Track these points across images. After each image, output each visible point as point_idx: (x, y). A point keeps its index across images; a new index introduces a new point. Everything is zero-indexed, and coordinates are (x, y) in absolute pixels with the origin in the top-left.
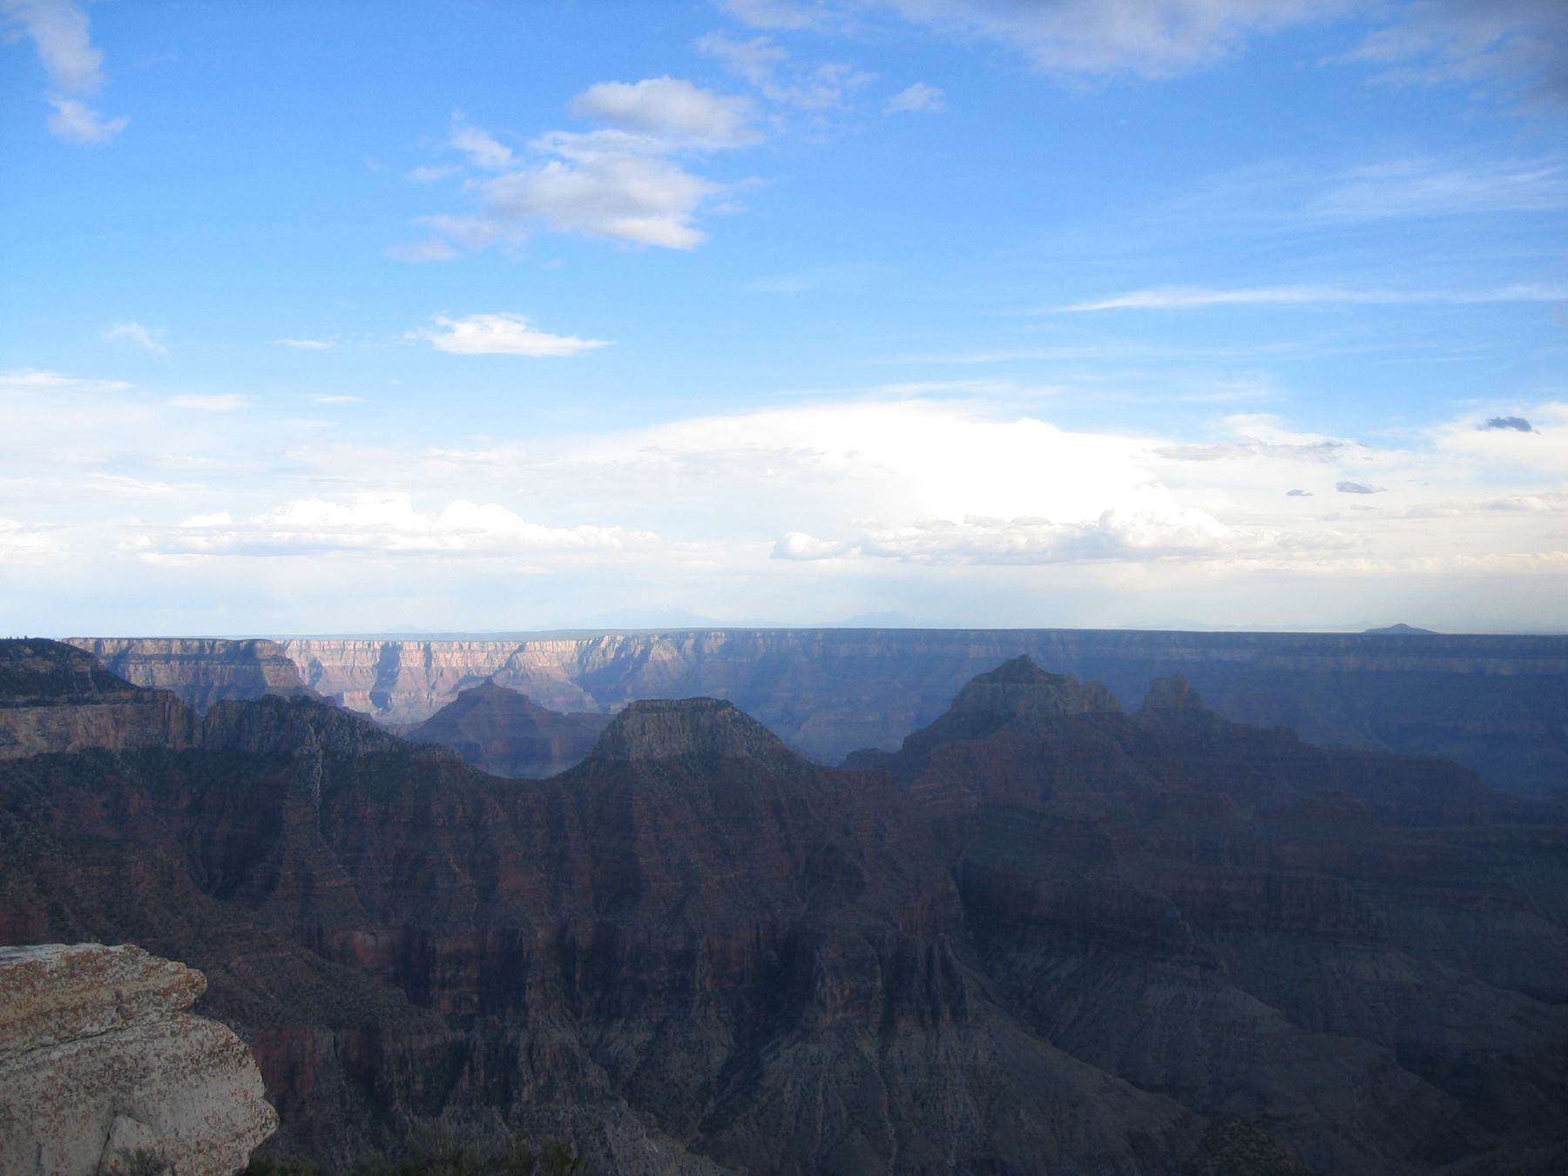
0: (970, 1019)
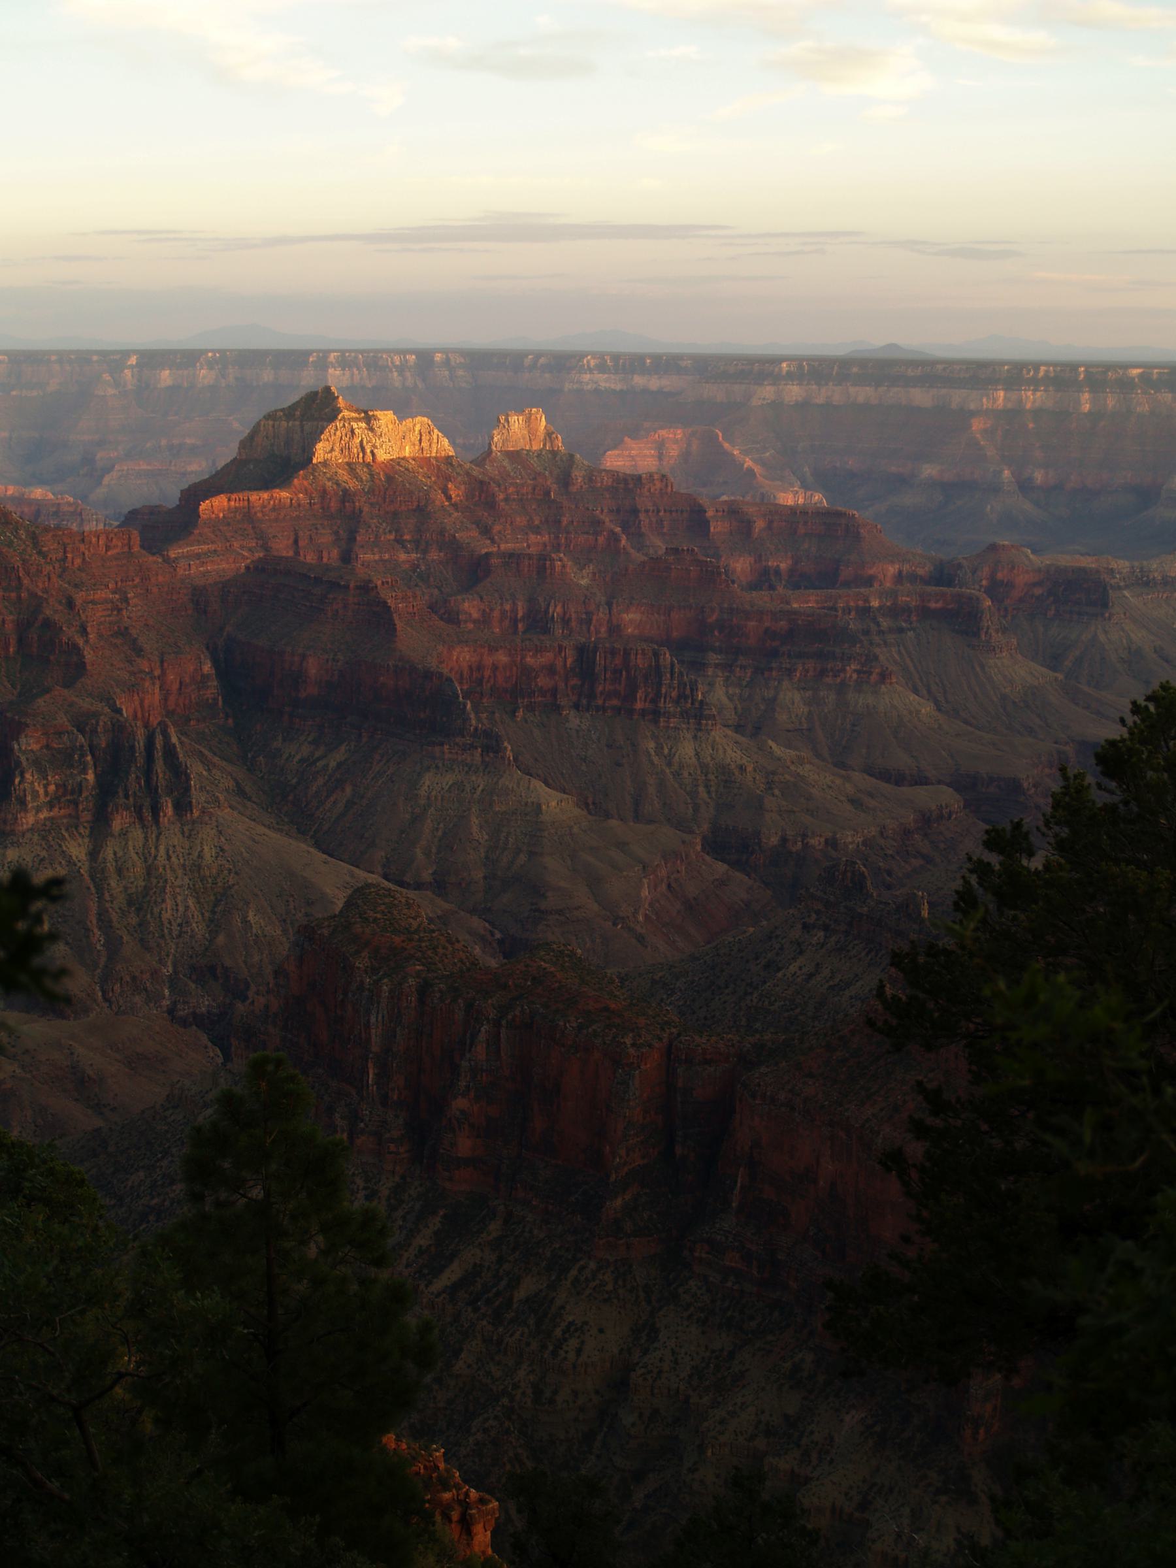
0: (196, 814)
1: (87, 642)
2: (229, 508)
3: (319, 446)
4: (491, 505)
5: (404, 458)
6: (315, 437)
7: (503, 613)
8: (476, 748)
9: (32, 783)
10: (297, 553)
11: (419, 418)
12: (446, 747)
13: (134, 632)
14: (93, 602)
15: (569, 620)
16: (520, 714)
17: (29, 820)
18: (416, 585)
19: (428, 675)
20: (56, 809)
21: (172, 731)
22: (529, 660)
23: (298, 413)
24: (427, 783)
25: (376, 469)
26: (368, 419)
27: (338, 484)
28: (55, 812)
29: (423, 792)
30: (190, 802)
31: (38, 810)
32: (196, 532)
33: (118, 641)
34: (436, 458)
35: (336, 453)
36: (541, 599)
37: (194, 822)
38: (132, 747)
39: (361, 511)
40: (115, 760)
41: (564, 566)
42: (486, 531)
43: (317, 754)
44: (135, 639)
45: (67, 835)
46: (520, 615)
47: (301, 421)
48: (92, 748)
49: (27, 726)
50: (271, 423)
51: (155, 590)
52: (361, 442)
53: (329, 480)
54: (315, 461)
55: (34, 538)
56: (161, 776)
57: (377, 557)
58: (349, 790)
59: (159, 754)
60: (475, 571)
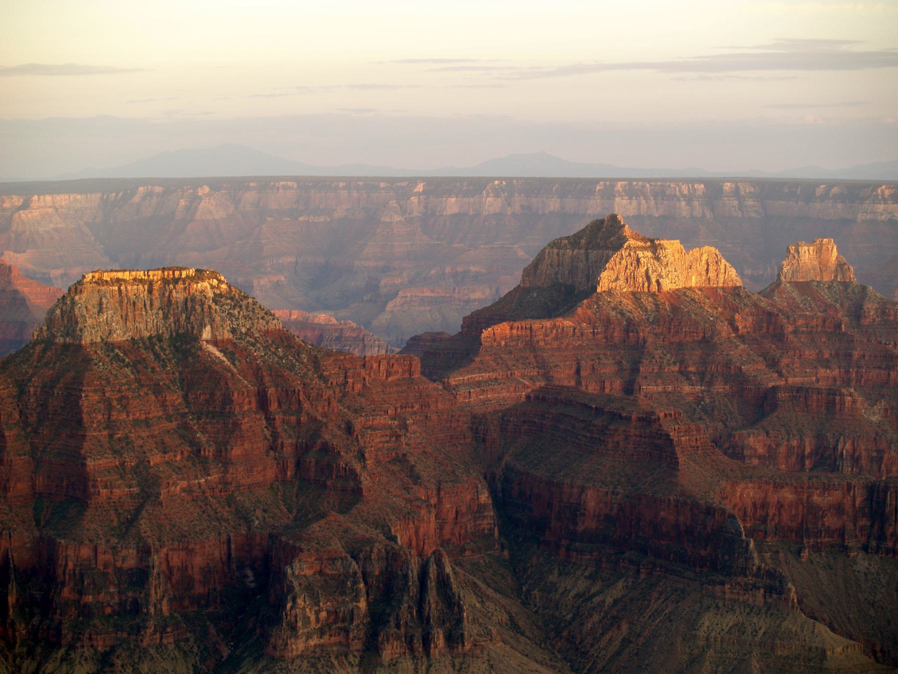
0: (468, 646)
1: (364, 467)
2: (511, 337)
3: (604, 275)
4: (779, 337)
5: (690, 289)
6: (601, 265)
7: (790, 449)
8: (758, 588)
9: (304, 608)
10: (579, 383)
11: (706, 248)
12: (727, 586)
13: (412, 460)
14: (372, 428)
15: (859, 458)
16: (805, 554)
17: (299, 646)
18: (700, 419)
19: (710, 511)
20: (327, 637)
21: (446, 561)
22: (816, 498)
23: (583, 241)
24: (707, 623)
25: (661, 299)
26: (654, 248)
27: (622, 314)
28: (325, 639)
29: (701, 633)
30: (462, 635)
31: (309, 636)
32: (477, 359)
33: (396, 468)
34: (723, 288)
35: (621, 282)
36: (829, 435)
37: (465, 655)
38: (406, 576)
39: (645, 342)
40: (387, 590)
41: (854, 402)
42: (773, 364)
43: (593, 590)
44: (413, 466)
45: (336, 663)
46: (808, 450)
47: (587, 249)
48: (365, 575)
49: (301, 550)
50: (556, 251)
51: (434, 417)
52: (647, 271)
53: (613, 309)
54: (599, 290)
55: (316, 362)
56: (433, 606)
57: (660, 389)
58: (625, 627)
59: (432, 584)
60: (762, 405)
